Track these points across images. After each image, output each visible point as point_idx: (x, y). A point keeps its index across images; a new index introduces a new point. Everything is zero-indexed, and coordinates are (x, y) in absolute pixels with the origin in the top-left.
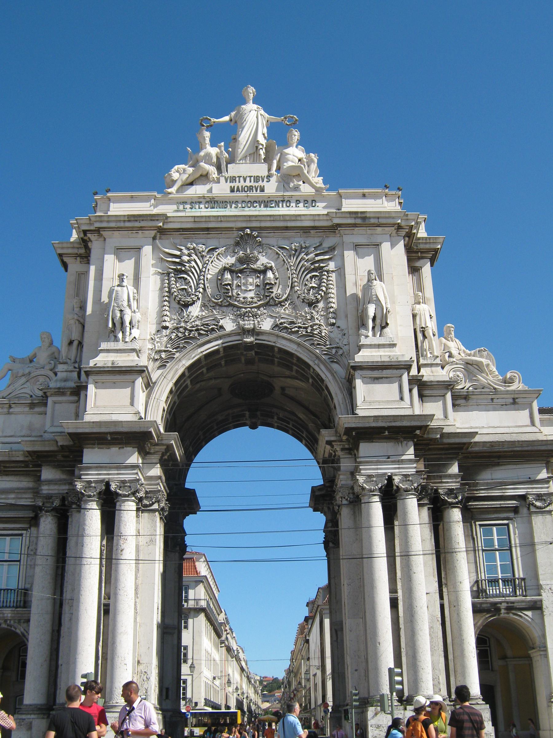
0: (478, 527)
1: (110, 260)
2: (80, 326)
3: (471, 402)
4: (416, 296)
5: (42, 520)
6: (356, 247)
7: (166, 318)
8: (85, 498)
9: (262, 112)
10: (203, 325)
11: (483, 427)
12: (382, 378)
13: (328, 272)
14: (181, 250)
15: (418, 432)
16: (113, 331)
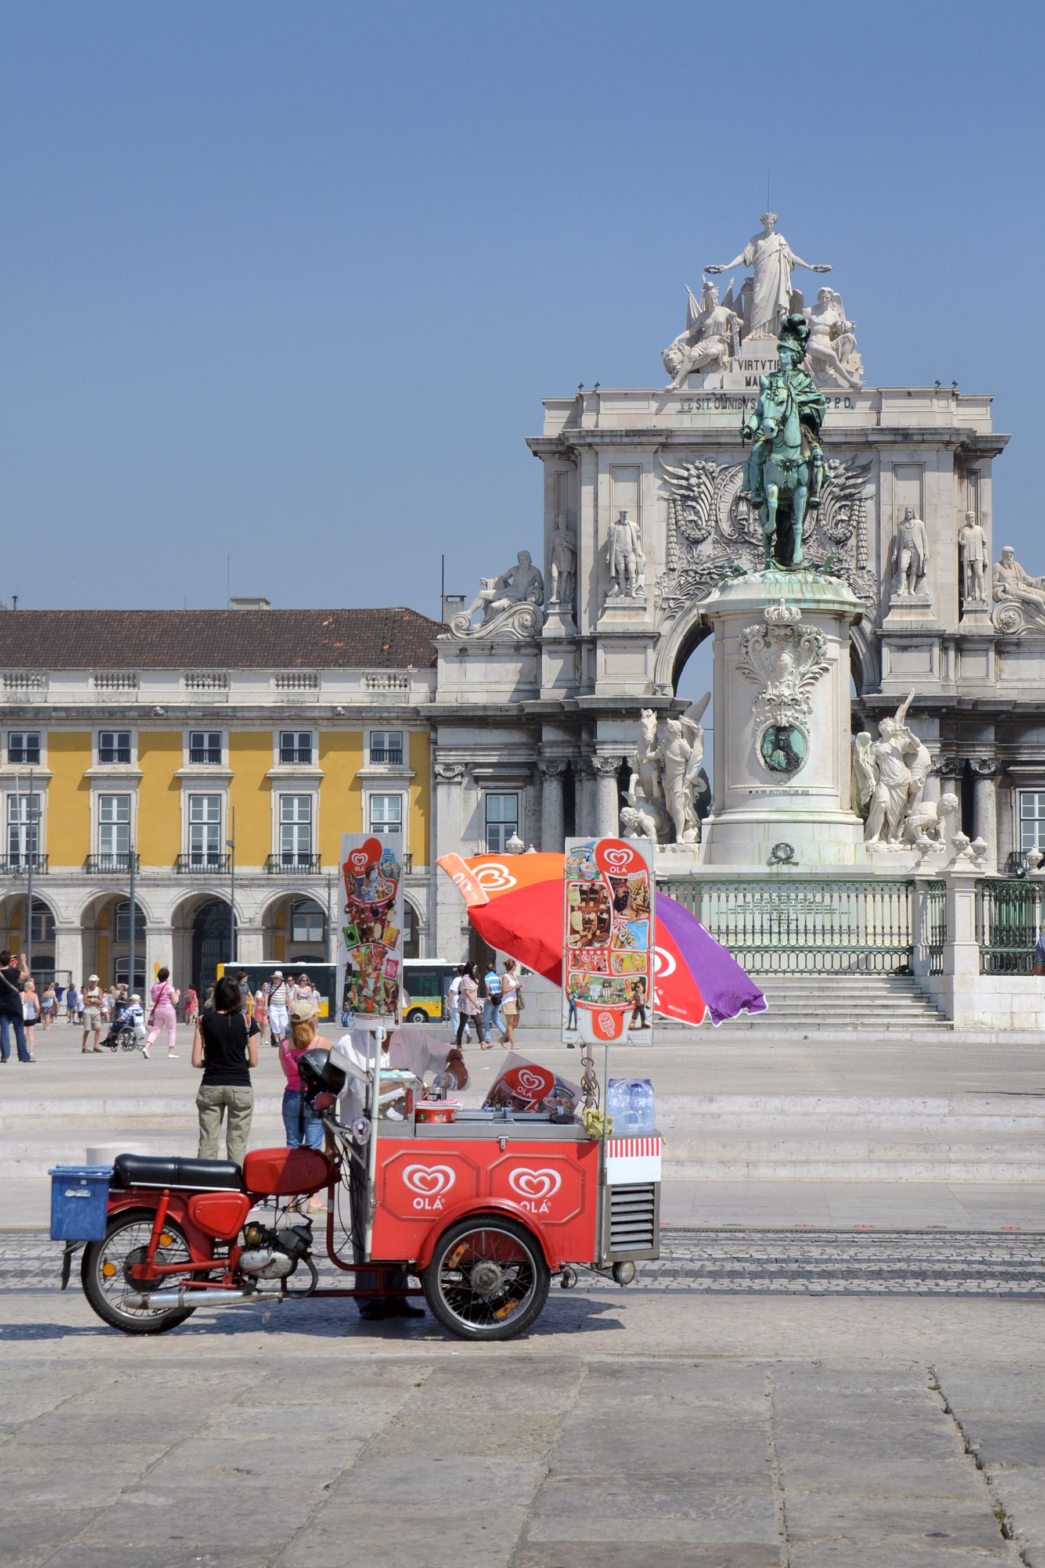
0: (1018, 794)
1: (604, 478)
2: (568, 555)
3: (1022, 649)
4: (968, 517)
5: (546, 785)
6: (895, 467)
7: (674, 559)
8: (601, 774)
9: (787, 250)
10: (716, 567)
11: (1034, 680)
12: (911, 647)
13: (860, 500)
14: (688, 470)
15: (944, 710)
16: (617, 578)
